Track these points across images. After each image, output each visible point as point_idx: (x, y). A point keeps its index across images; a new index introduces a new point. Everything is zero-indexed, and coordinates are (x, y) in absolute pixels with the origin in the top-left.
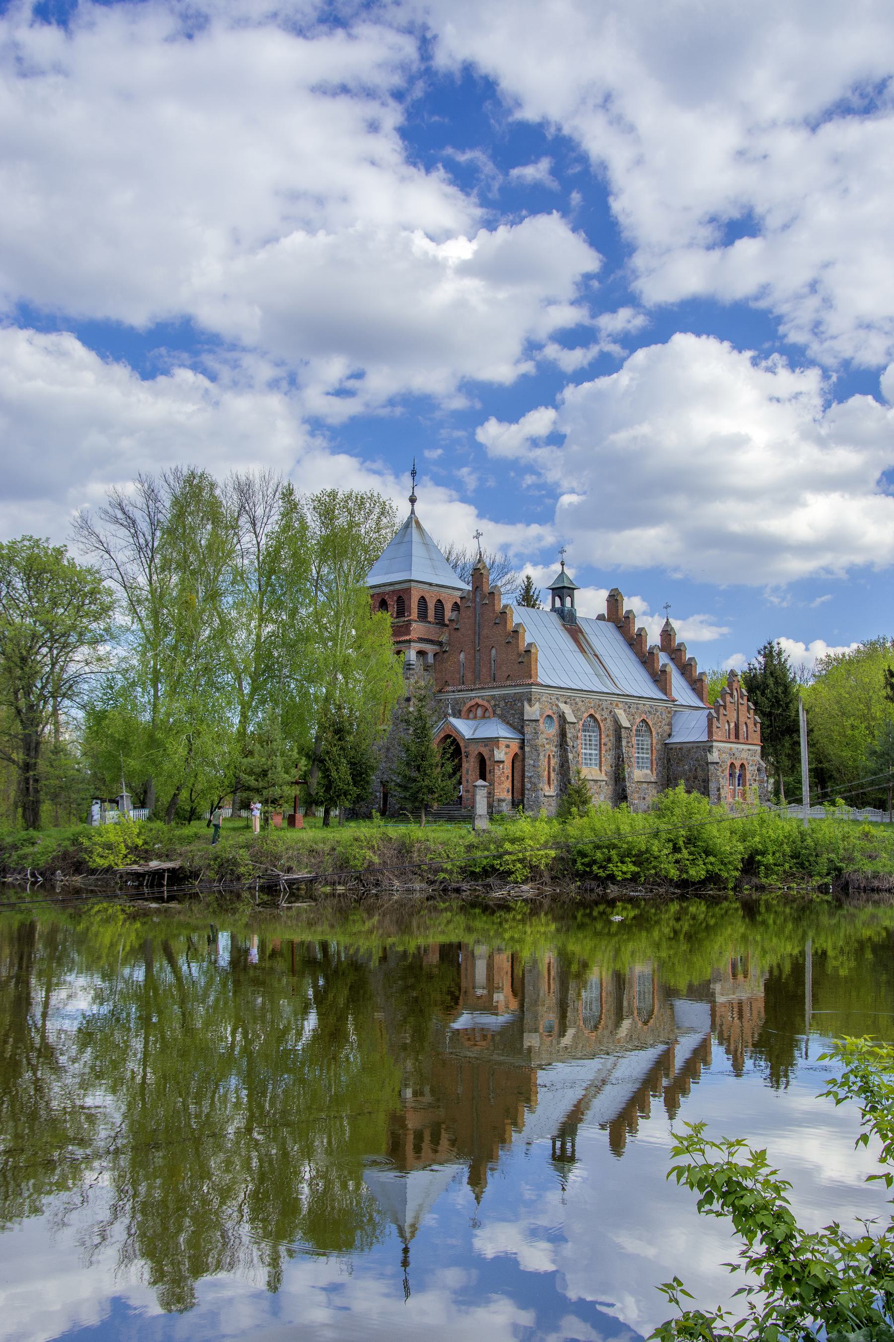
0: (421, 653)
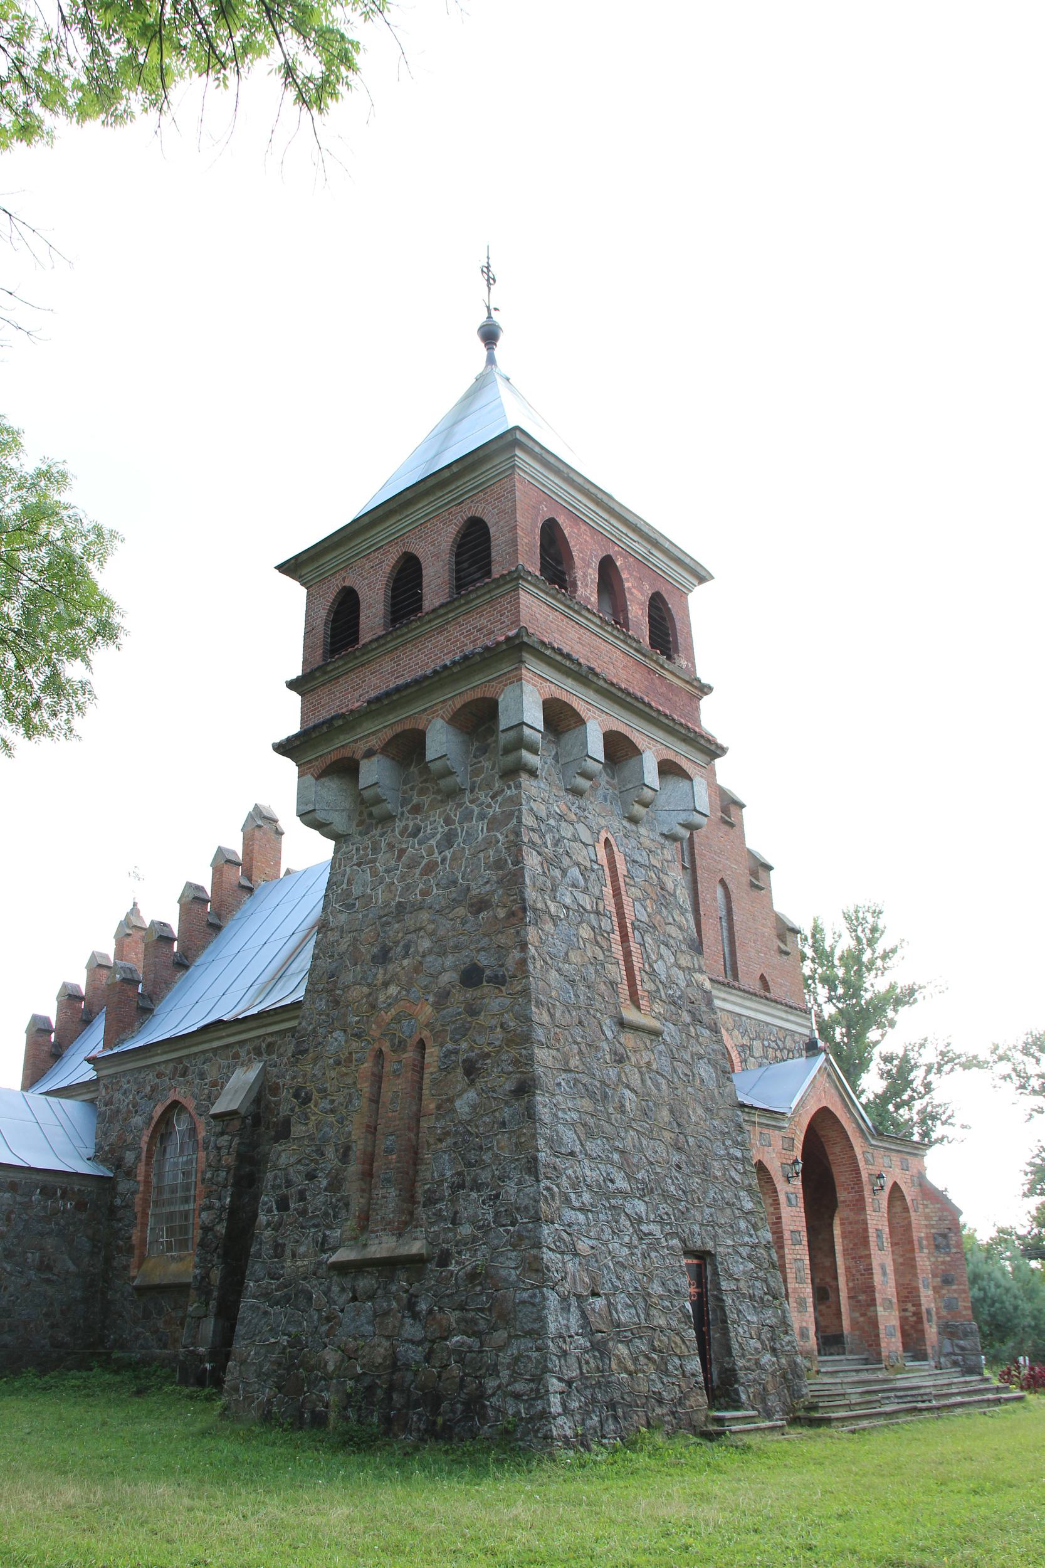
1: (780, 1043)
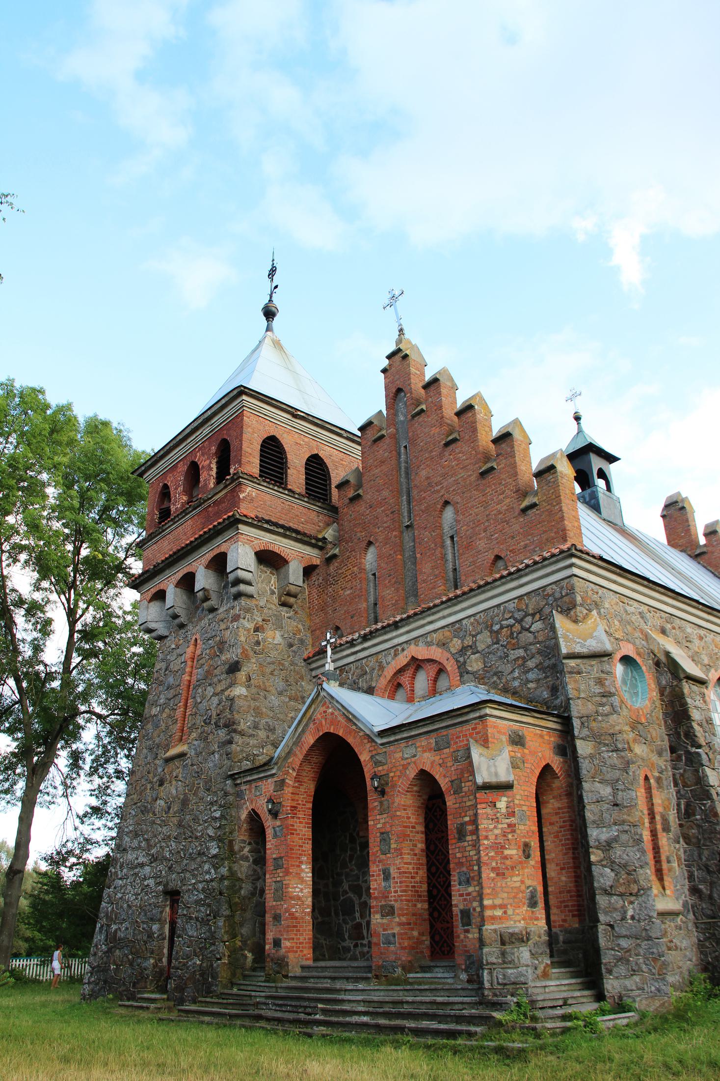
0: (268, 559)
1: (516, 616)
